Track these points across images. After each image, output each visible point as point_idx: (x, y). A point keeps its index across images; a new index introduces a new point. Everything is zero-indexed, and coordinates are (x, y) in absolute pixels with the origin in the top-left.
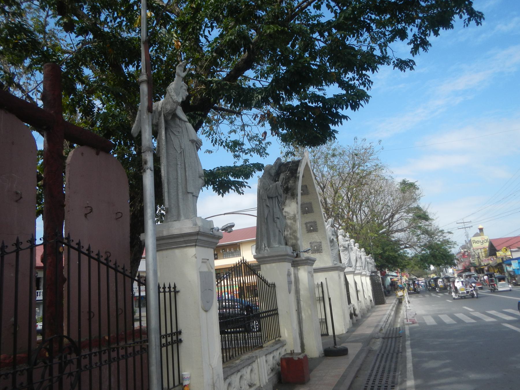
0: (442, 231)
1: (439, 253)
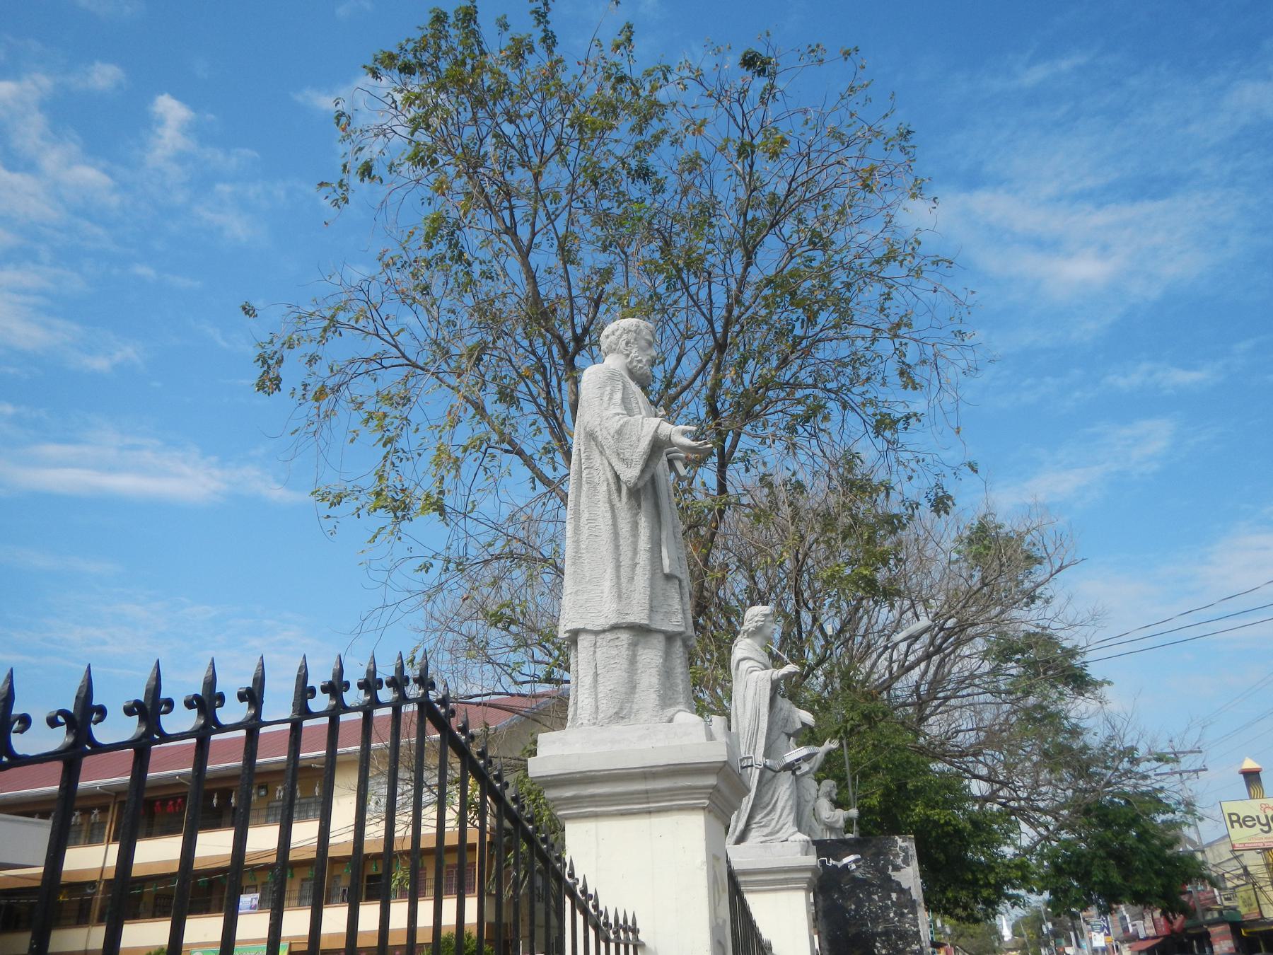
0: (1130, 753)
1: (1141, 837)
